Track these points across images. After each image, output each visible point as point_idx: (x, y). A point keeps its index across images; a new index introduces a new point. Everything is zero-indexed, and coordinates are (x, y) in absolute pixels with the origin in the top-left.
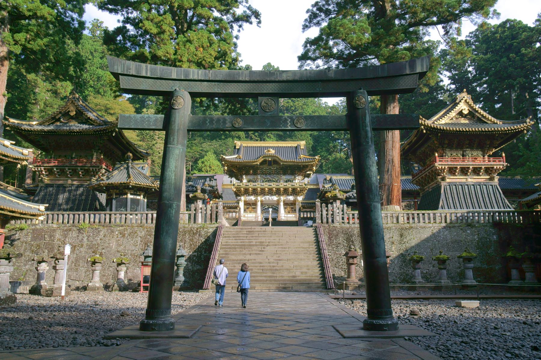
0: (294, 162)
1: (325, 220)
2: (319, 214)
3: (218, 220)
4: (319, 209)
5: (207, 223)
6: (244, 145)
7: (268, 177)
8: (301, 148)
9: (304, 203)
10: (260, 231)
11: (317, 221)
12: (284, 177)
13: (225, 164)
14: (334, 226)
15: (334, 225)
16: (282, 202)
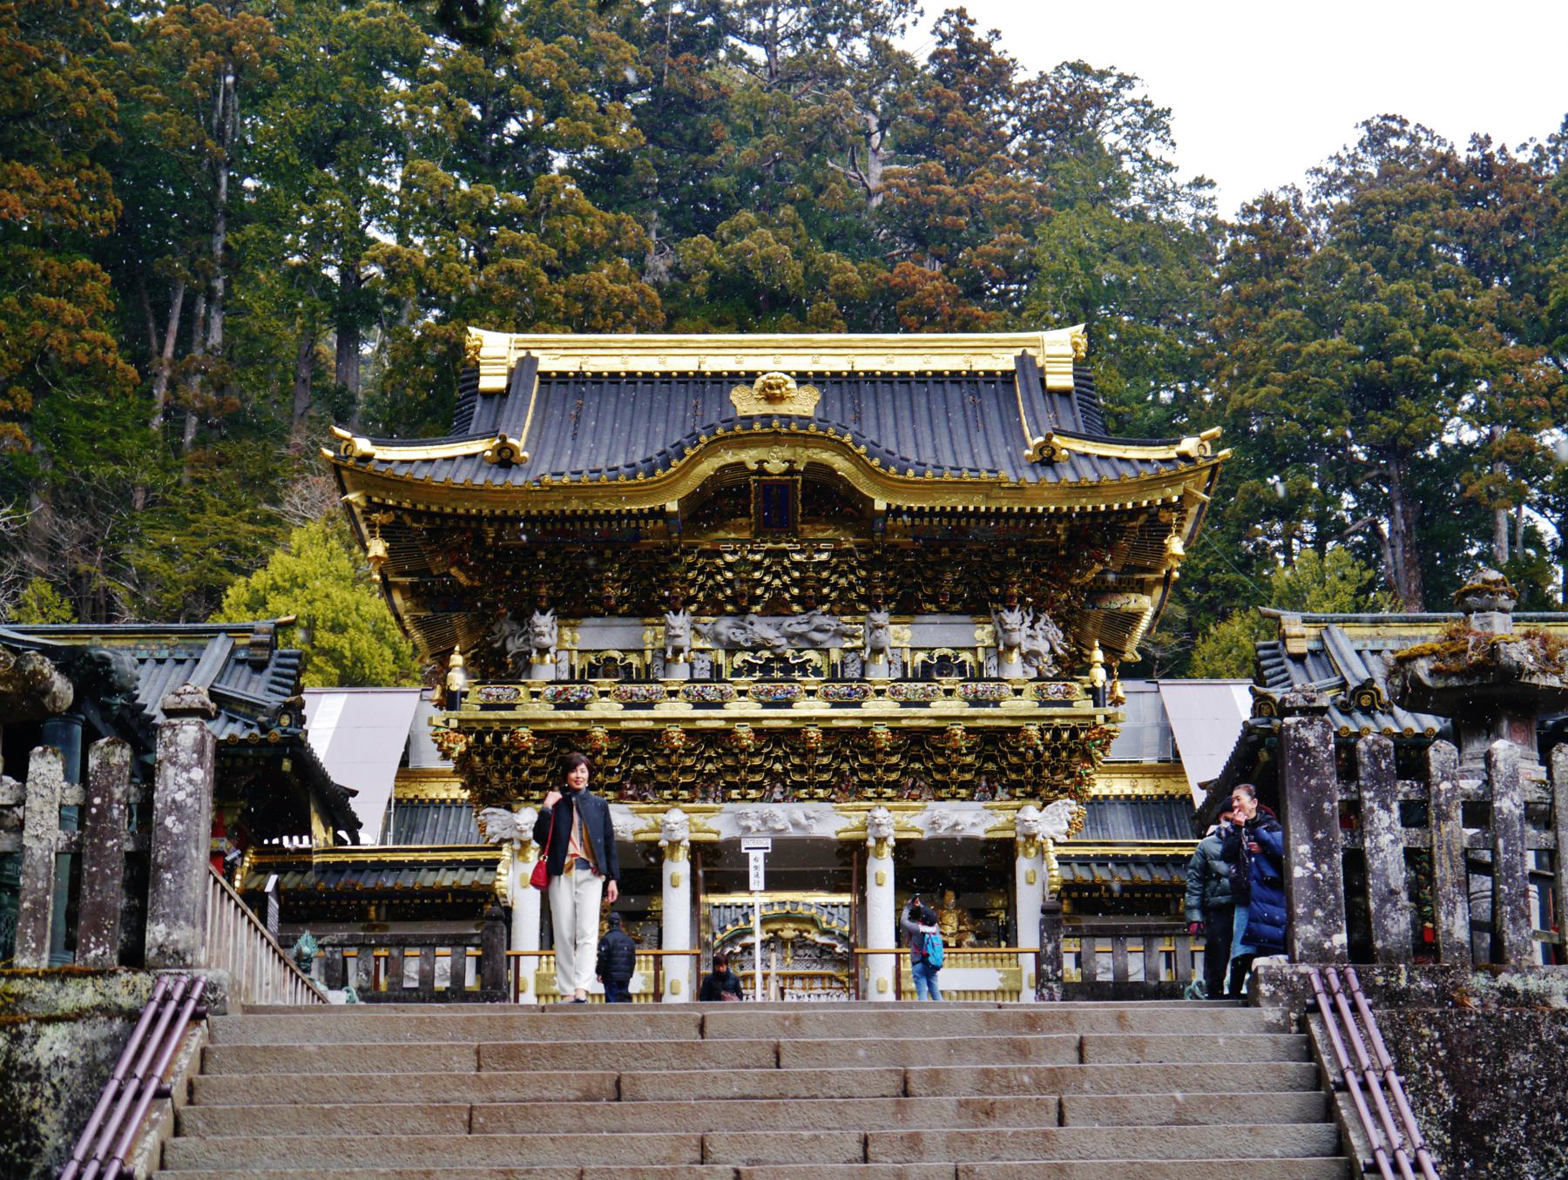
0: (991, 488)
1: (1397, 925)
2: (1321, 853)
3: (156, 932)
4: (1322, 792)
5: (23, 961)
6: (549, 363)
7: (763, 629)
8: (1052, 382)
9: (1084, 861)
10: (644, 1052)
11: (1306, 932)
12: (900, 636)
13: (371, 508)
14: (1508, 992)
15: (1504, 979)
16: (887, 852)
